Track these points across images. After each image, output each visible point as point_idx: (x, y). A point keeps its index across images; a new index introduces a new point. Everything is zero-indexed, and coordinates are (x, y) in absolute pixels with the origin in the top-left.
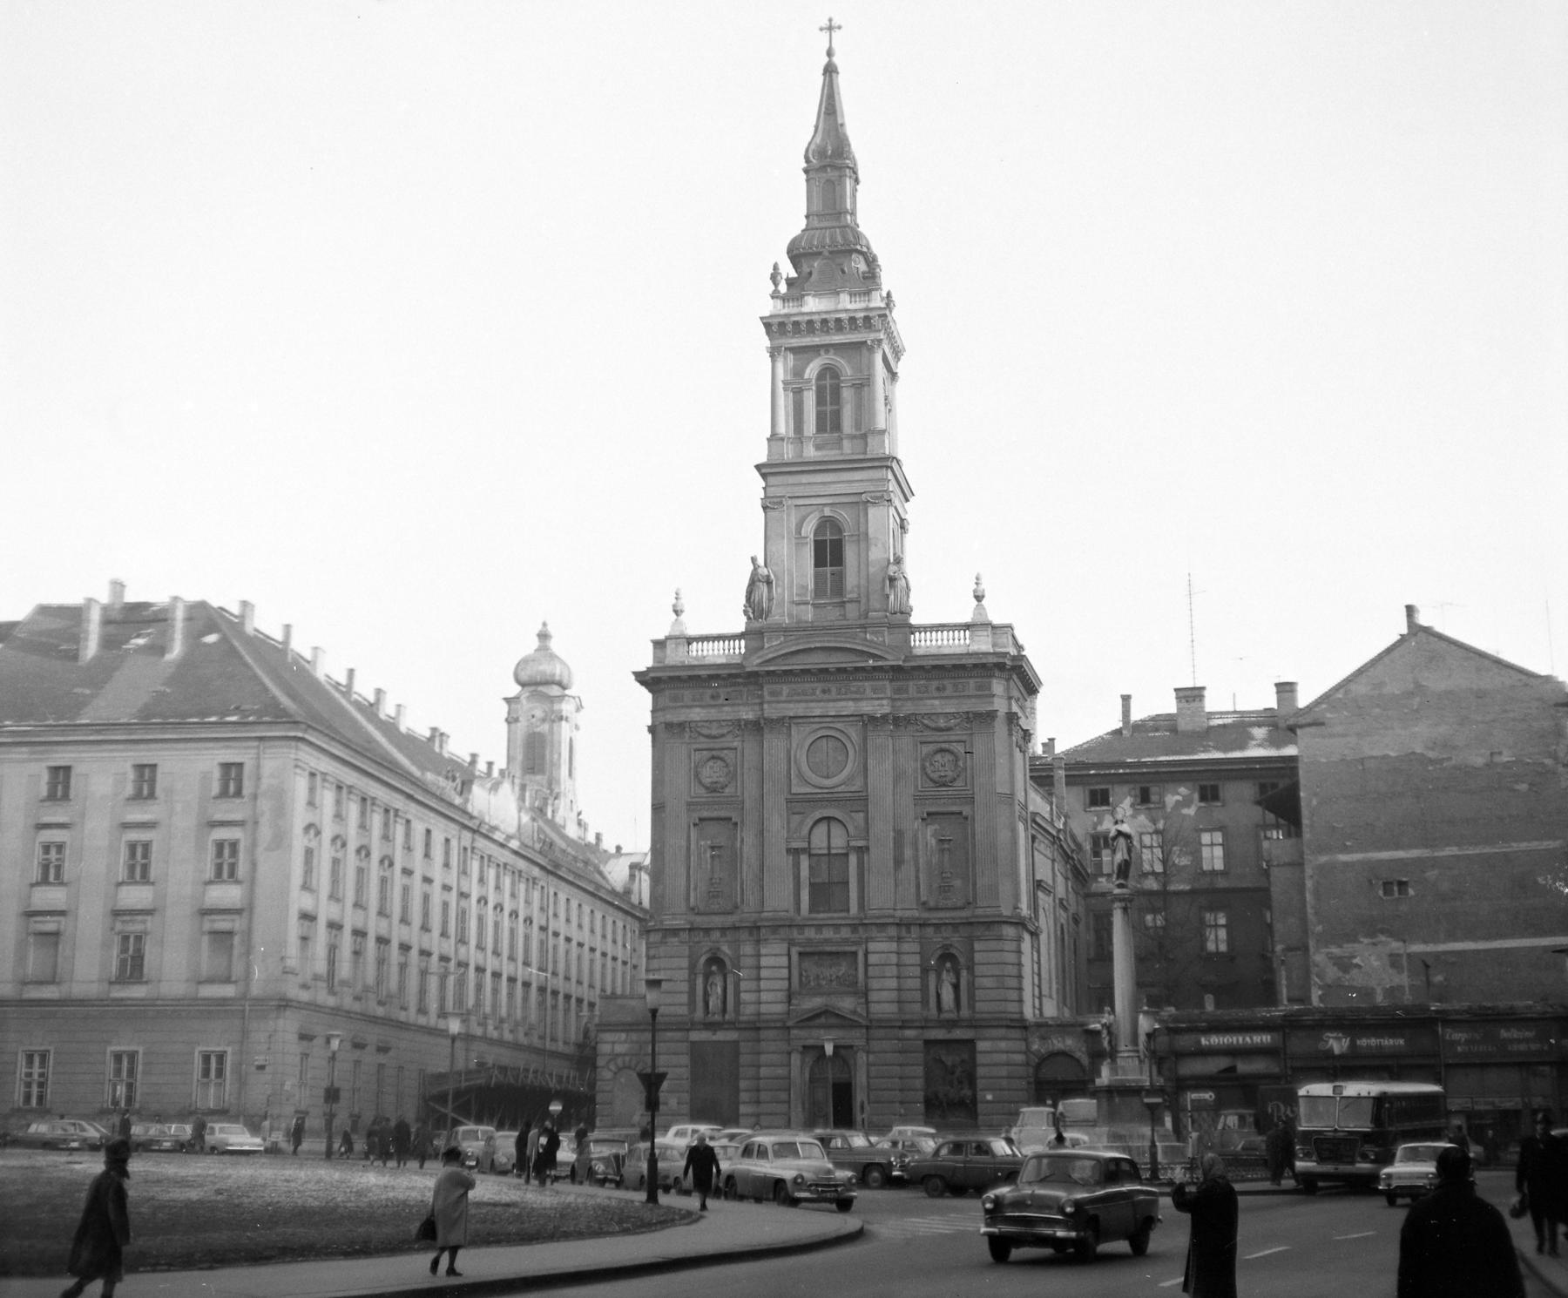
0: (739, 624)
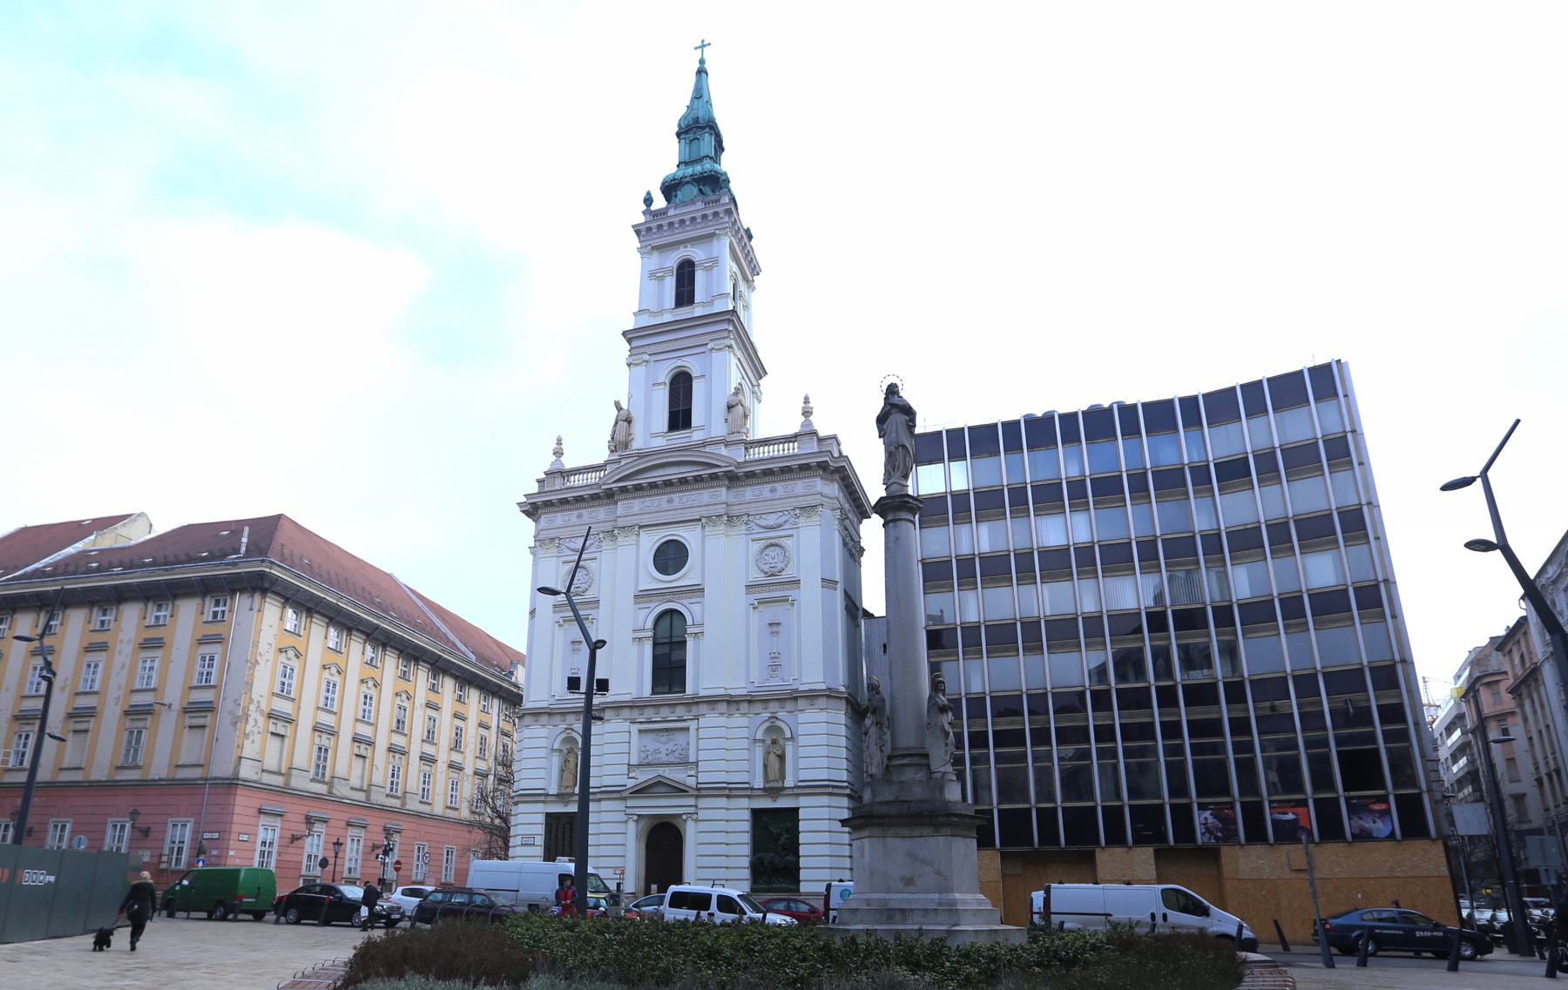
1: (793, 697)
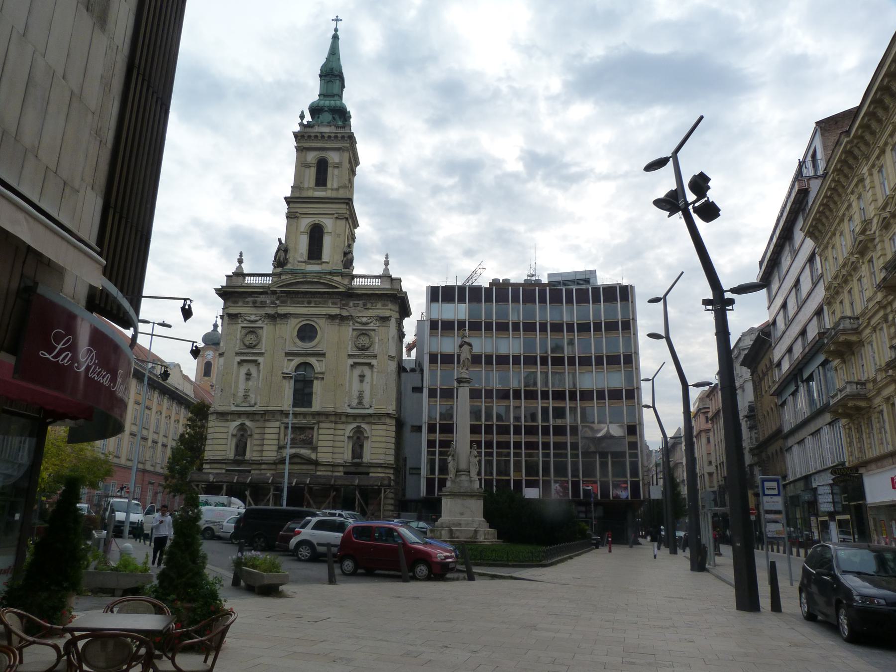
0: (270, 269)
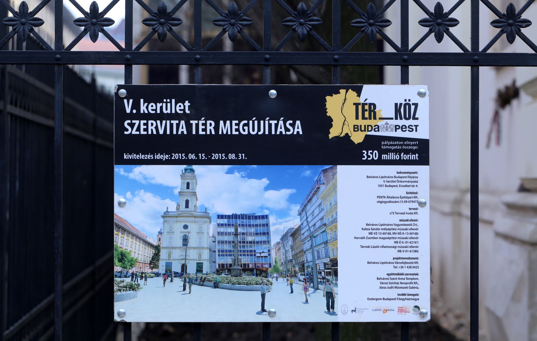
0: (175, 210)
1: (203, 248)
